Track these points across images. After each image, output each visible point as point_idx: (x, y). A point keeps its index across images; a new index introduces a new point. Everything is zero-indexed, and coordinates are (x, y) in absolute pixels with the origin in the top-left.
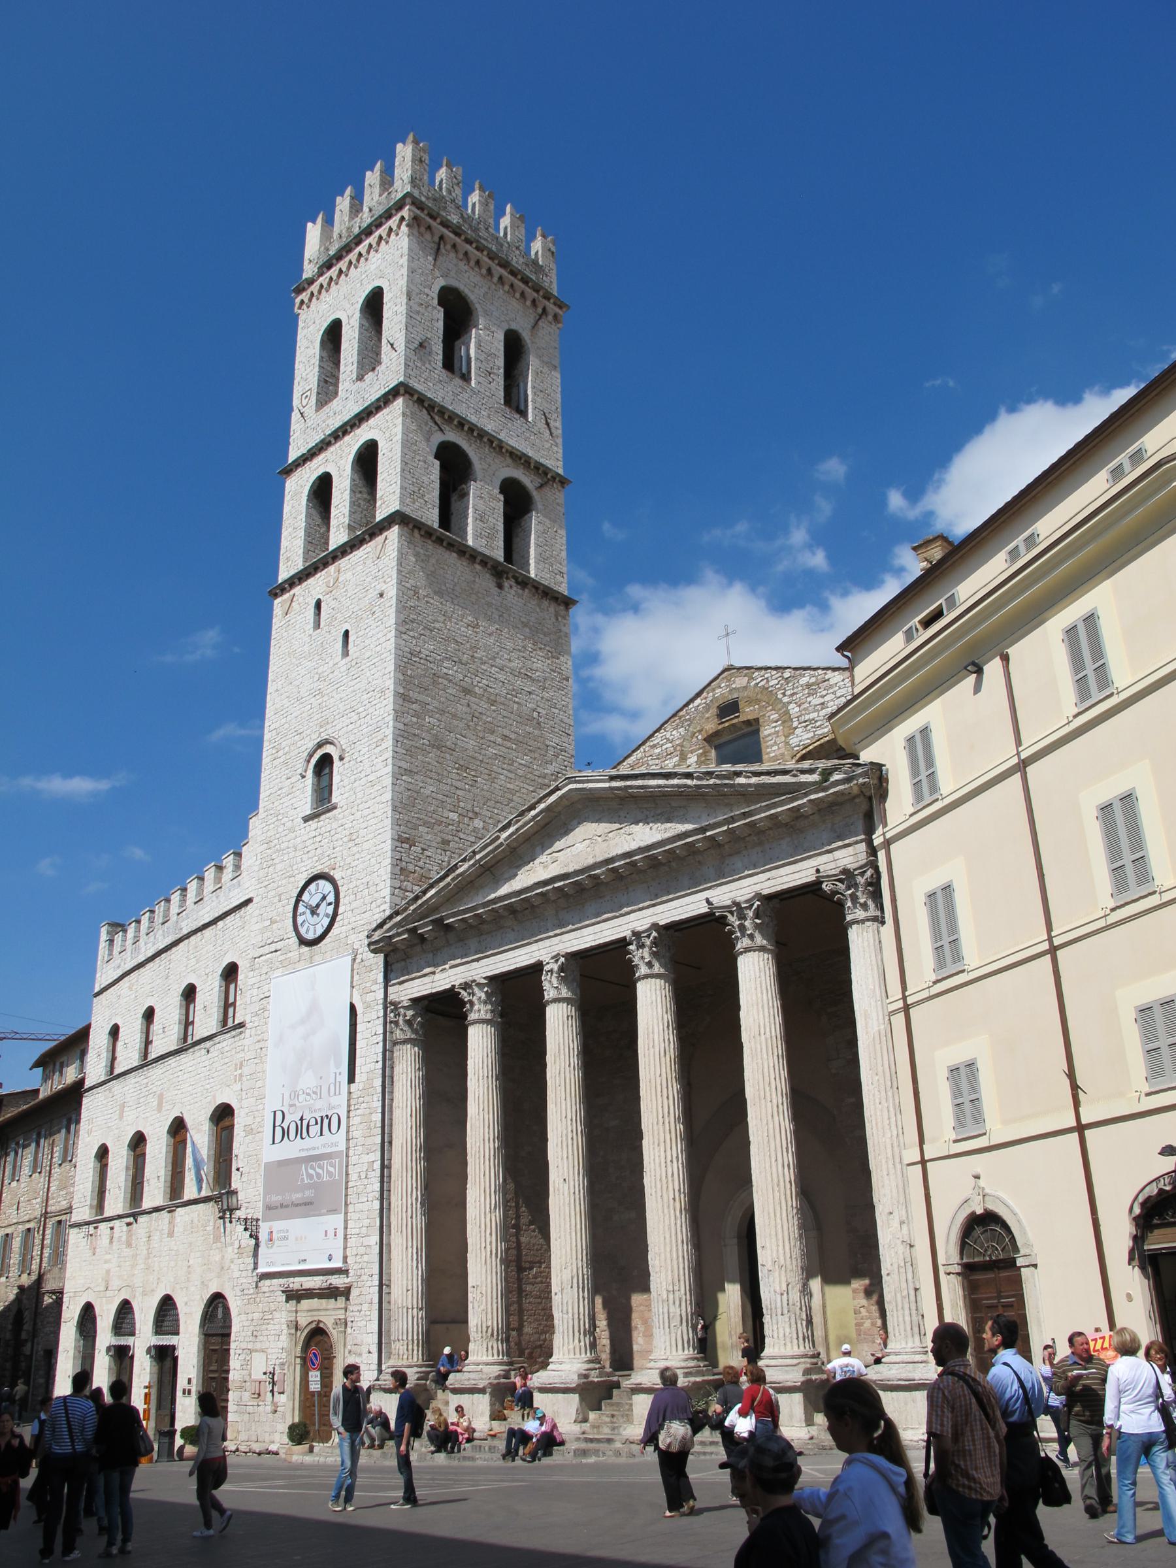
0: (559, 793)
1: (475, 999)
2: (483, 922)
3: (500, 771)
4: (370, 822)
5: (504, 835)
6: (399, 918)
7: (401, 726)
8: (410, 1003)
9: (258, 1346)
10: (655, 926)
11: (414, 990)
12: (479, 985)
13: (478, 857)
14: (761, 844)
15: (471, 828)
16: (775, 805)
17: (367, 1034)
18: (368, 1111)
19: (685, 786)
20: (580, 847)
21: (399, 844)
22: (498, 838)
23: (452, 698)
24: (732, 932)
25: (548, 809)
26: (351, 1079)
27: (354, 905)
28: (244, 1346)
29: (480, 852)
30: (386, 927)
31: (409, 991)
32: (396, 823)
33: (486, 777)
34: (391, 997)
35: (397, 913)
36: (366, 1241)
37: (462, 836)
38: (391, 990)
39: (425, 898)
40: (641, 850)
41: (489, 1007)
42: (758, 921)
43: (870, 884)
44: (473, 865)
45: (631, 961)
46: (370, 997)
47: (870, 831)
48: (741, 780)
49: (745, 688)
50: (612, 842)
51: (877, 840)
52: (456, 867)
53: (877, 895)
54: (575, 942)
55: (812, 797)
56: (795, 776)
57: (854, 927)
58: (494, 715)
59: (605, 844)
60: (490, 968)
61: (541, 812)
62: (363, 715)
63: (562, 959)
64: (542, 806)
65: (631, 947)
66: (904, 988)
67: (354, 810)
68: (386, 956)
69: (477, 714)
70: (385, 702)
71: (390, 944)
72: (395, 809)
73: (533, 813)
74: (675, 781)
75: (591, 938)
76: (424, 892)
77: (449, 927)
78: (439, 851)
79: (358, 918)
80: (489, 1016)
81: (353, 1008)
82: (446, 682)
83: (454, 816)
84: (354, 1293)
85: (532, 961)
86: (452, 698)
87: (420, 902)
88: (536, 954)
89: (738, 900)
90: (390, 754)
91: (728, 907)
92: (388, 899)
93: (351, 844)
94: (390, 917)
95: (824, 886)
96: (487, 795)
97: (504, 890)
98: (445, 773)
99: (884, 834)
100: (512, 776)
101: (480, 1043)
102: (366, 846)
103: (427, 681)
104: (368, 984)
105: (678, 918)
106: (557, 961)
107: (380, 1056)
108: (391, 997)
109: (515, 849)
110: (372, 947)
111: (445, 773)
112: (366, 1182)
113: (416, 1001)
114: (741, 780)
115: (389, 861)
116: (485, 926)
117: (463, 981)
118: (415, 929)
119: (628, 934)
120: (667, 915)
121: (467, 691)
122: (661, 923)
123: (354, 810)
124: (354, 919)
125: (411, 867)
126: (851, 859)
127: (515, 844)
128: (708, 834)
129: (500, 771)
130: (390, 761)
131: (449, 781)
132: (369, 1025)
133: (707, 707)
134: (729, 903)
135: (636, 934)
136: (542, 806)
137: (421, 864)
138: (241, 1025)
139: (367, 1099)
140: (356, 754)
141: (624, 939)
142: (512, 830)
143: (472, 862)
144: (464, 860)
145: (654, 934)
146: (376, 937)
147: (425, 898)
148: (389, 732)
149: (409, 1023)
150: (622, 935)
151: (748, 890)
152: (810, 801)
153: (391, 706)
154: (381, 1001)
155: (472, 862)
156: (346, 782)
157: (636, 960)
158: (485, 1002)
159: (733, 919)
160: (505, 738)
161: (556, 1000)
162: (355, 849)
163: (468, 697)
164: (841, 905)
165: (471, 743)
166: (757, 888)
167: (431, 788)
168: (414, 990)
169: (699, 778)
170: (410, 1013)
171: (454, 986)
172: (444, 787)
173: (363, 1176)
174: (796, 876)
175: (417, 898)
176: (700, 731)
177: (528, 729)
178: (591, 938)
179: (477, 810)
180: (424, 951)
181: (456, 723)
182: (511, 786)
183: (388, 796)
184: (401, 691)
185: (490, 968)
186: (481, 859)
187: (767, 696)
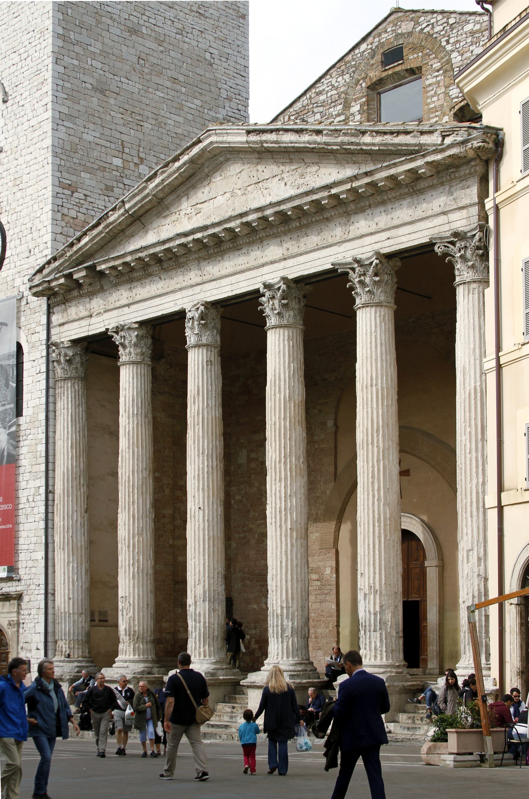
0: (201, 146)
1: (127, 342)
2: (132, 270)
3: (168, 115)
4: (33, 168)
5: (152, 185)
6: (57, 264)
7: (62, 70)
8: (69, 344)
10: (284, 279)
11: (73, 332)
12: (129, 328)
13: (127, 206)
14: (383, 203)
15: (136, 174)
16: (395, 165)
17: (33, 372)
18: (34, 442)
19: (315, 143)
20: (220, 200)
21: (60, 190)
22: (145, 188)
23: (116, 39)
24: (352, 288)
25: (192, 161)
26: (19, 412)
27: (19, 250)
29: (129, 201)
30: (45, 272)
31: (68, 333)
32: (58, 169)
33: (153, 122)
34: (54, 338)
35: (55, 259)
37: (126, 182)
38: (53, 331)
39: (79, 245)
40: (271, 205)
41: (139, 350)
42: (377, 279)
43: (478, 248)
44: (123, 215)
45: (262, 312)
46: (35, 338)
47: (483, 194)
48: (367, 139)
50: (250, 196)
51: (489, 204)
52: (106, 216)
53: (485, 257)
54: (215, 292)
55: (430, 159)
56: (415, 137)
57: (461, 287)
58: (162, 56)
59: (244, 197)
60: (140, 313)
61: (184, 164)
62: (24, 56)
63: (202, 308)
64: (185, 158)
65: (264, 299)
66: (499, 348)
67: (18, 155)
68: (48, 299)
69: (143, 56)
70: (44, 44)
71: (51, 289)
72: (55, 155)
73: (177, 164)
74: (306, 138)
75: (228, 288)
76: (79, 240)
77: (102, 273)
78: (102, 197)
79: (23, 262)
80: (139, 359)
81: (19, 347)
82: (109, 22)
83: (117, 162)
85: (177, 309)
86: (116, 39)
87: (75, 248)
88: (179, 302)
89: (359, 257)
90: (49, 99)
91: (350, 264)
92: (49, 244)
93: (15, 189)
94: (49, 263)
95: (436, 248)
96: (155, 141)
98: (108, 118)
99: (494, 199)
100: (181, 120)
101: (130, 382)
102: (29, 191)
103: (91, 21)
104: (33, 325)
105: (306, 273)
107: (44, 392)
108: (54, 338)
109: (162, 199)
110: (34, 290)
111: (108, 118)
113: (75, 342)
114: (367, 139)
115: (50, 207)
116: (135, 275)
117: (115, 325)
118: (70, 275)
119: (261, 286)
120: (296, 269)
121: (133, 31)
122: (290, 277)
123: (18, 155)
124: (18, 263)
125: (73, 213)
126: (464, 222)
127: (161, 195)
128: (333, 191)
129: (168, 115)
130: (50, 106)
131: (113, 127)
132: (34, 364)
134: (350, 260)
135: (268, 286)
136: (185, 158)
137: (83, 210)
139: (33, 431)
140: (18, 98)
141: (257, 291)
142: (157, 180)
143: (122, 211)
144: (114, 209)
145: (284, 287)
146: (37, 280)
147: (79, 245)
148: (48, 75)
149: (69, 362)
150: (256, 287)
151: (369, 248)
152: (427, 163)
153: (50, 49)
154: (44, 342)
155: (122, 211)
156: (10, 126)
157: (268, 311)
158: (136, 345)
159: (355, 278)
160: (175, 80)
161: (197, 346)
162: (19, 194)
163: (134, 37)
164: (451, 267)
165: (134, 86)
166: (377, 247)
167: (94, 134)
168: (73, 332)
169: (327, 135)
170: (70, 353)
171: (107, 330)
172: (107, 132)
174: (413, 236)
175: (72, 245)
176: (364, 79)
177: (198, 71)
178: (228, 288)
179: (142, 155)
180: (81, 296)
181: (118, 65)
182: (179, 131)
183: (48, 142)
184: (61, 32)
185: (140, 313)
186: (130, 208)
187: (431, 43)
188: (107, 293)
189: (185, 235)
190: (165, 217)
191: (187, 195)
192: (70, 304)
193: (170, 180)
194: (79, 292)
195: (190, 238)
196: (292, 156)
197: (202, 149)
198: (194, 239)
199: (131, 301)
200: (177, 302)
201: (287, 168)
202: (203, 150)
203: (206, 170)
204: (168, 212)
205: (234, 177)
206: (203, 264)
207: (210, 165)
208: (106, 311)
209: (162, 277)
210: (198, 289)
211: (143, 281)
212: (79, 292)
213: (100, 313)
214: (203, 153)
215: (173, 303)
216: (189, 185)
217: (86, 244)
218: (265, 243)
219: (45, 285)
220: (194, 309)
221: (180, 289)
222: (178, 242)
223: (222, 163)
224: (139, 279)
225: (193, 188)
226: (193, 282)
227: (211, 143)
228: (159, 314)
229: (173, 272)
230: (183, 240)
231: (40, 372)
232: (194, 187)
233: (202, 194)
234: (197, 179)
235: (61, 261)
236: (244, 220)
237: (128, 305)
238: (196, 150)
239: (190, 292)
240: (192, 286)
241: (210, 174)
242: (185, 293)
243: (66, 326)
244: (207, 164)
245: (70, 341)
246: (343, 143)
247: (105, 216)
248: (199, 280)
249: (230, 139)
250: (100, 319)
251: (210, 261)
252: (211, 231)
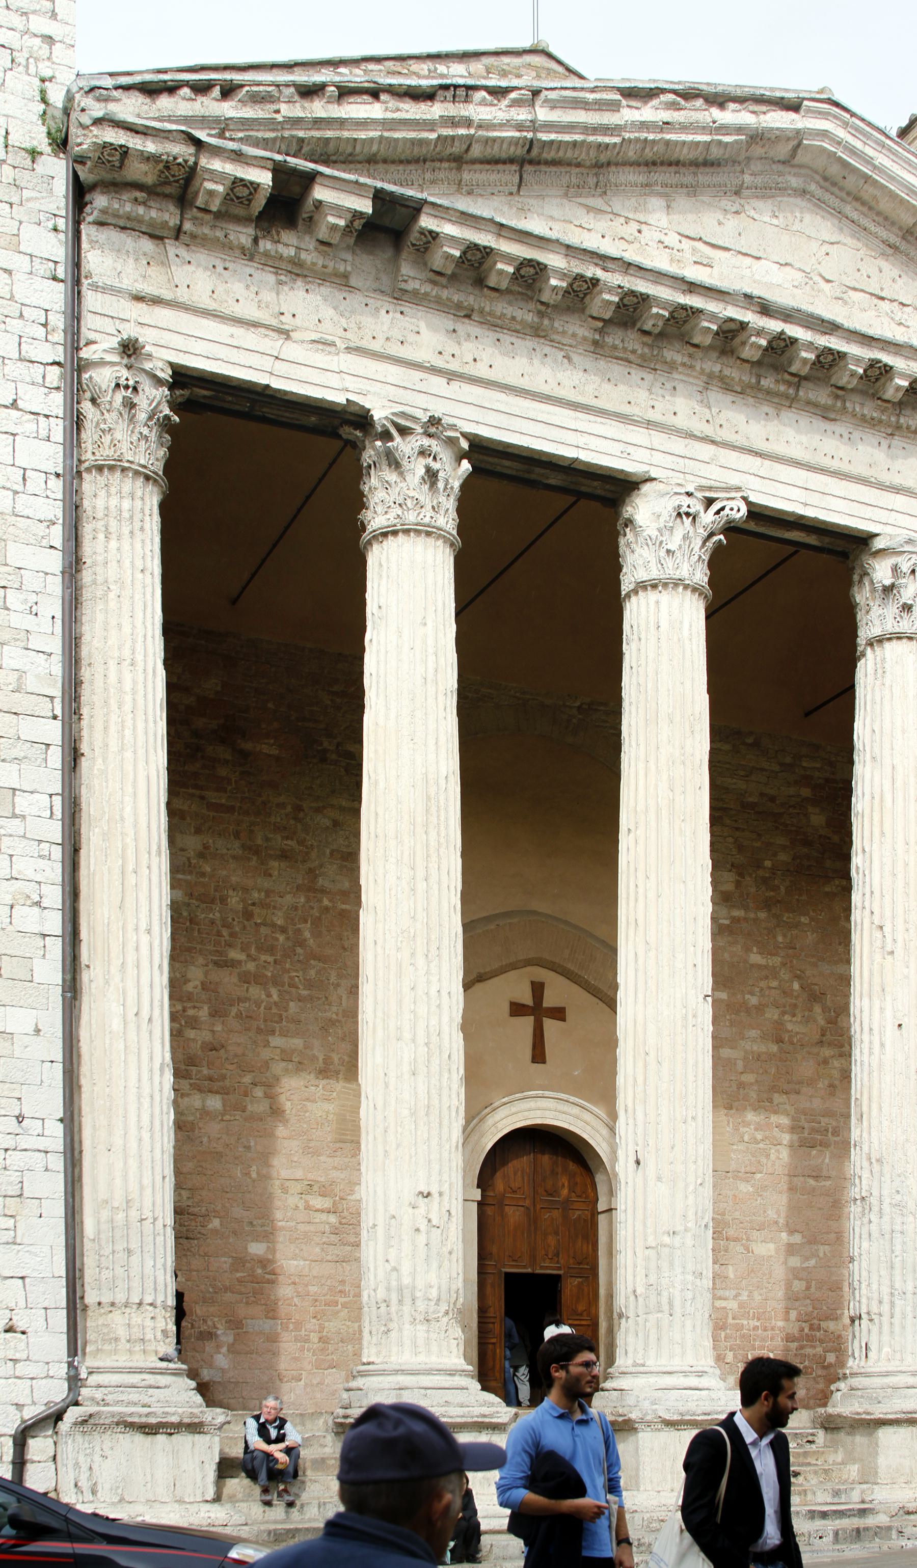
60: (492, 418)
106: (709, 502)
180: (249, 254)
185: (492, 418)
188: (356, 300)
190: (589, 209)
191: (668, 194)
192: (182, 251)
193: (684, 137)
194: (256, 241)
195: (775, 326)
197: (798, 132)
198: (782, 333)
199: (454, 366)
200: (630, 449)
202: (797, 138)
203: (747, 178)
204: (598, 202)
205: (814, 245)
206: (715, 396)
207: (762, 173)
209: (575, 358)
210: (705, 451)
211: (507, 338)
212: (256, 241)
213: (333, 344)
214: (788, 139)
215: (621, 446)
216: (689, 179)
217: (363, 124)
219: (181, 151)
220: (699, 495)
221: (649, 424)
222: (732, 312)
223: (782, 190)
224: (495, 324)
225: (688, 195)
226: (681, 422)
227: (824, 134)
228: (569, 453)
229: (617, 369)
232: (692, 190)
233: (712, 220)
234: (717, 179)
235: (249, 112)
237: (452, 376)
238: (778, 120)
239: (678, 445)
240: (690, 435)
241: (746, 192)
242: (658, 439)
244: (756, 166)
245: (171, 364)
247: (461, 92)
248: (699, 427)
249: (882, 159)
250: (320, 358)
251: (738, 399)
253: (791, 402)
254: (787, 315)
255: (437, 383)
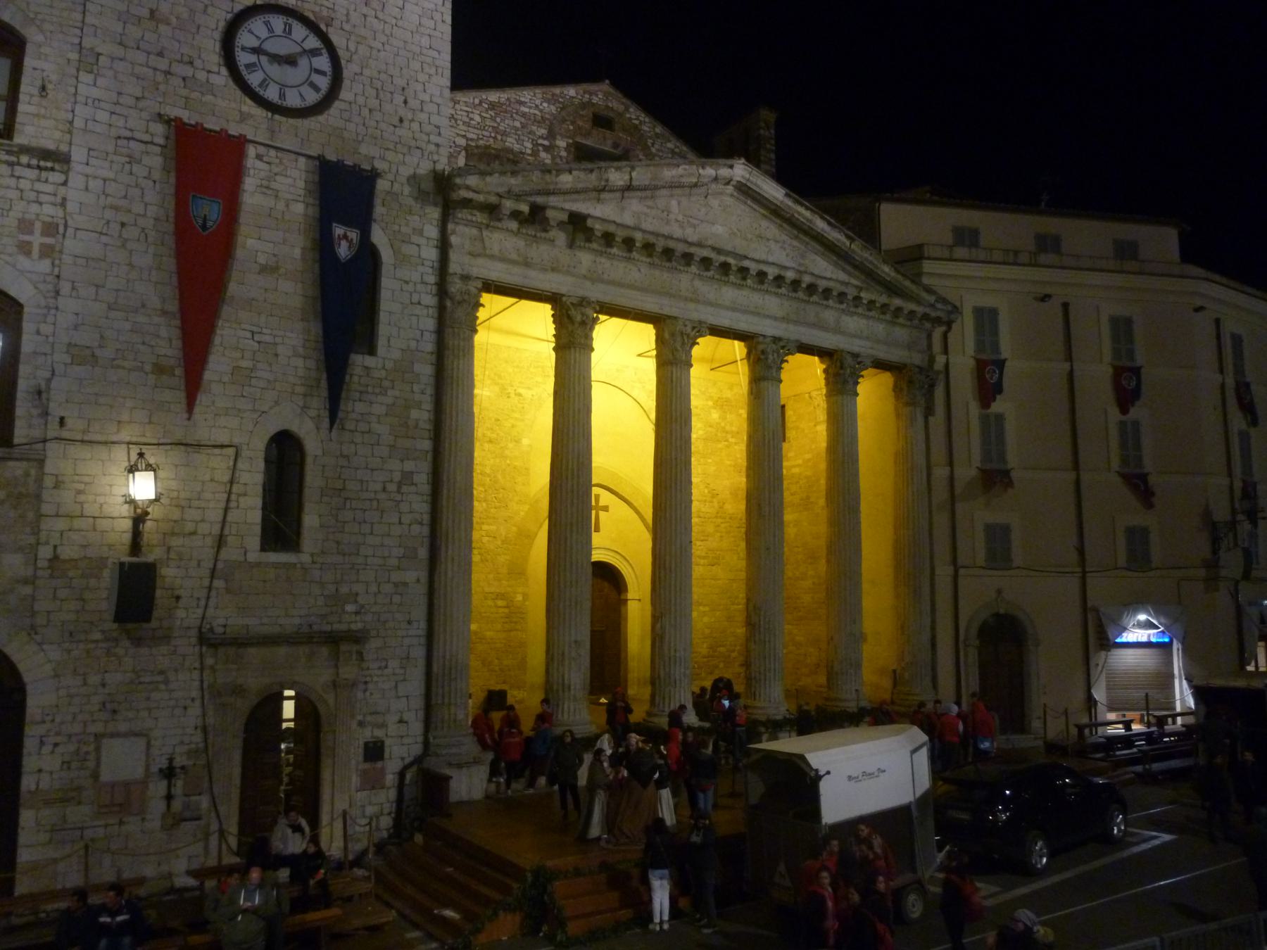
6: (513, 181)
9: (123, 727)
28: (77, 728)
36: (396, 576)
49: (621, 115)
84: (373, 644)
97: (628, 219)
112: (398, 497)
132: (405, 287)
133: (584, 106)
138: (55, 159)
173: (392, 487)
180: (517, 233)
189: (719, 251)
190: (648, 207)
195: (722, 258)
196: (801, 236)
201: (789, 241)
208: (553, 270)
218: (767, 297)
224: (612, 257)
230: (713, 255)
231: (419, 303)
236: (782, 273)
243: (480, 261)
246: (866, 259)
252: (746, 263)
253: (726, 283)
254: (728, 253)
255: (588, 283)
